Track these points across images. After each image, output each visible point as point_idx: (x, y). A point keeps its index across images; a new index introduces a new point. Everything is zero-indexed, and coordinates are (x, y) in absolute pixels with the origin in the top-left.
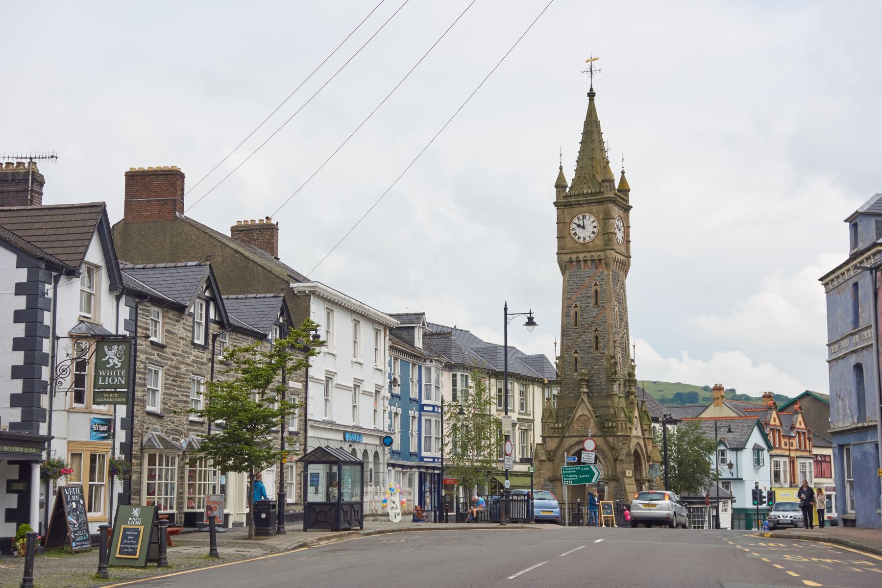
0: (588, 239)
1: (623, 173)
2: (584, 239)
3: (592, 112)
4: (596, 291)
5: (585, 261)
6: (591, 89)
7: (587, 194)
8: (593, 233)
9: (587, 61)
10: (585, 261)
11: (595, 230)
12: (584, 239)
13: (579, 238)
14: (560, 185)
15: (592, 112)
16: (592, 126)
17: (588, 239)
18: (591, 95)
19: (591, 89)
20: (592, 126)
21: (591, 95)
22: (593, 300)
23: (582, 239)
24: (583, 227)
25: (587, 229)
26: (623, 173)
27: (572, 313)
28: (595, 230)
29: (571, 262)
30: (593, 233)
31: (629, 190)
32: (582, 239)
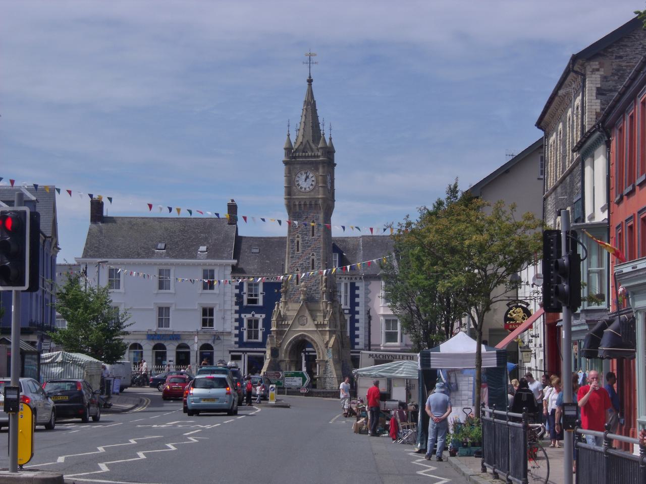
0: (308, 189)
1: (331, 139)
2: (305, 189)
3: (310, 93)
6: (310, 77)
8: (312, 185)
11: (313, 183)
12: (305, 189)
13: (301, 188)
14: (289, 150)
15: (310, 93)
16: (311, 105)
17: (308, 189)
18: (310, 81)
19: (310, 77)
20: (311, 105)
21: (310, 81)
22: (311, 232)
23: (303, 189)
25: (306, 183)
26: (331, 139)
27: (296, 242)
28: (313, 183)
30: (312, 185)
31: (334, 152)
32: (303, 189)
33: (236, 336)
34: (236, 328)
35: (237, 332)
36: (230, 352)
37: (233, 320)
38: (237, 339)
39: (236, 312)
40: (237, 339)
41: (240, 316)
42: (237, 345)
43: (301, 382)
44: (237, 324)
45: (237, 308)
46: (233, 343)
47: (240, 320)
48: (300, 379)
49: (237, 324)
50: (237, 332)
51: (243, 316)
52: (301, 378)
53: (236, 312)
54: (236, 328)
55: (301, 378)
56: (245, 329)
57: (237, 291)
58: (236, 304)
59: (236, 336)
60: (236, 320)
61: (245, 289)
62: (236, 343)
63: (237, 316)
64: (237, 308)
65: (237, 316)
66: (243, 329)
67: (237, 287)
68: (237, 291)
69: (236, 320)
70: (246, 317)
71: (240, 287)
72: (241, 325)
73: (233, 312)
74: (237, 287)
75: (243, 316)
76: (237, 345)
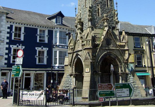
33: (6, 59)
34: (6, 54)
35: (7, 56)
36: (2, 70)
37: (5, 49)
38: (6, 61)
39: (7, 43)
40: (6, 61)
41: (9, 46)
42: (6, 66)
43: (128, 93)
44: (7, 51)
45: (8, 41)
46: (4, 64)
47: (9, 49)
48: (127, 90)
49: (7, 51)
50: (7, 56)
51: (11, 46)
52: (128, 89)
53: (7, 43)
54: (6, 54)
55: (128, 89)
56: (12, 55)
57: (9, 30)
58: (8, 38)
59: (6, 59)
60: (7, 49)
61: (14, 30)
62: (5, 64)
63: (7, 46)
64: (8, 41)
65: (7, 46)
66: (10, 55)
67: (8, 28)
68: (9, 30)
69: (7, 49)
70: (13, 47)
71: (11, 28)
72: (10, 52)
73: (5, 43)
74: (8, 28)
75: (11, 46)
76: (6, 66)
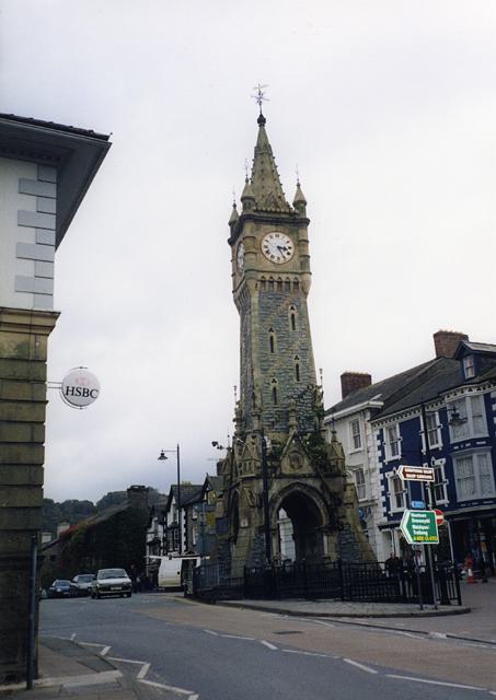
3: (262, 135)
4: (293, 316)
5: (272, 282)
6: (261, 116)
7: (271, 211)
9: (255, 88)
10: (280, 283)
12: (279, 258)
13: (272, 257)
15: (262, 135)
16: (263, 151)
18: (262, 121)
19: (261, 116)
20: (263, 151)
21: (262, 121)
24: (279, 248)
29: (263, 282)
